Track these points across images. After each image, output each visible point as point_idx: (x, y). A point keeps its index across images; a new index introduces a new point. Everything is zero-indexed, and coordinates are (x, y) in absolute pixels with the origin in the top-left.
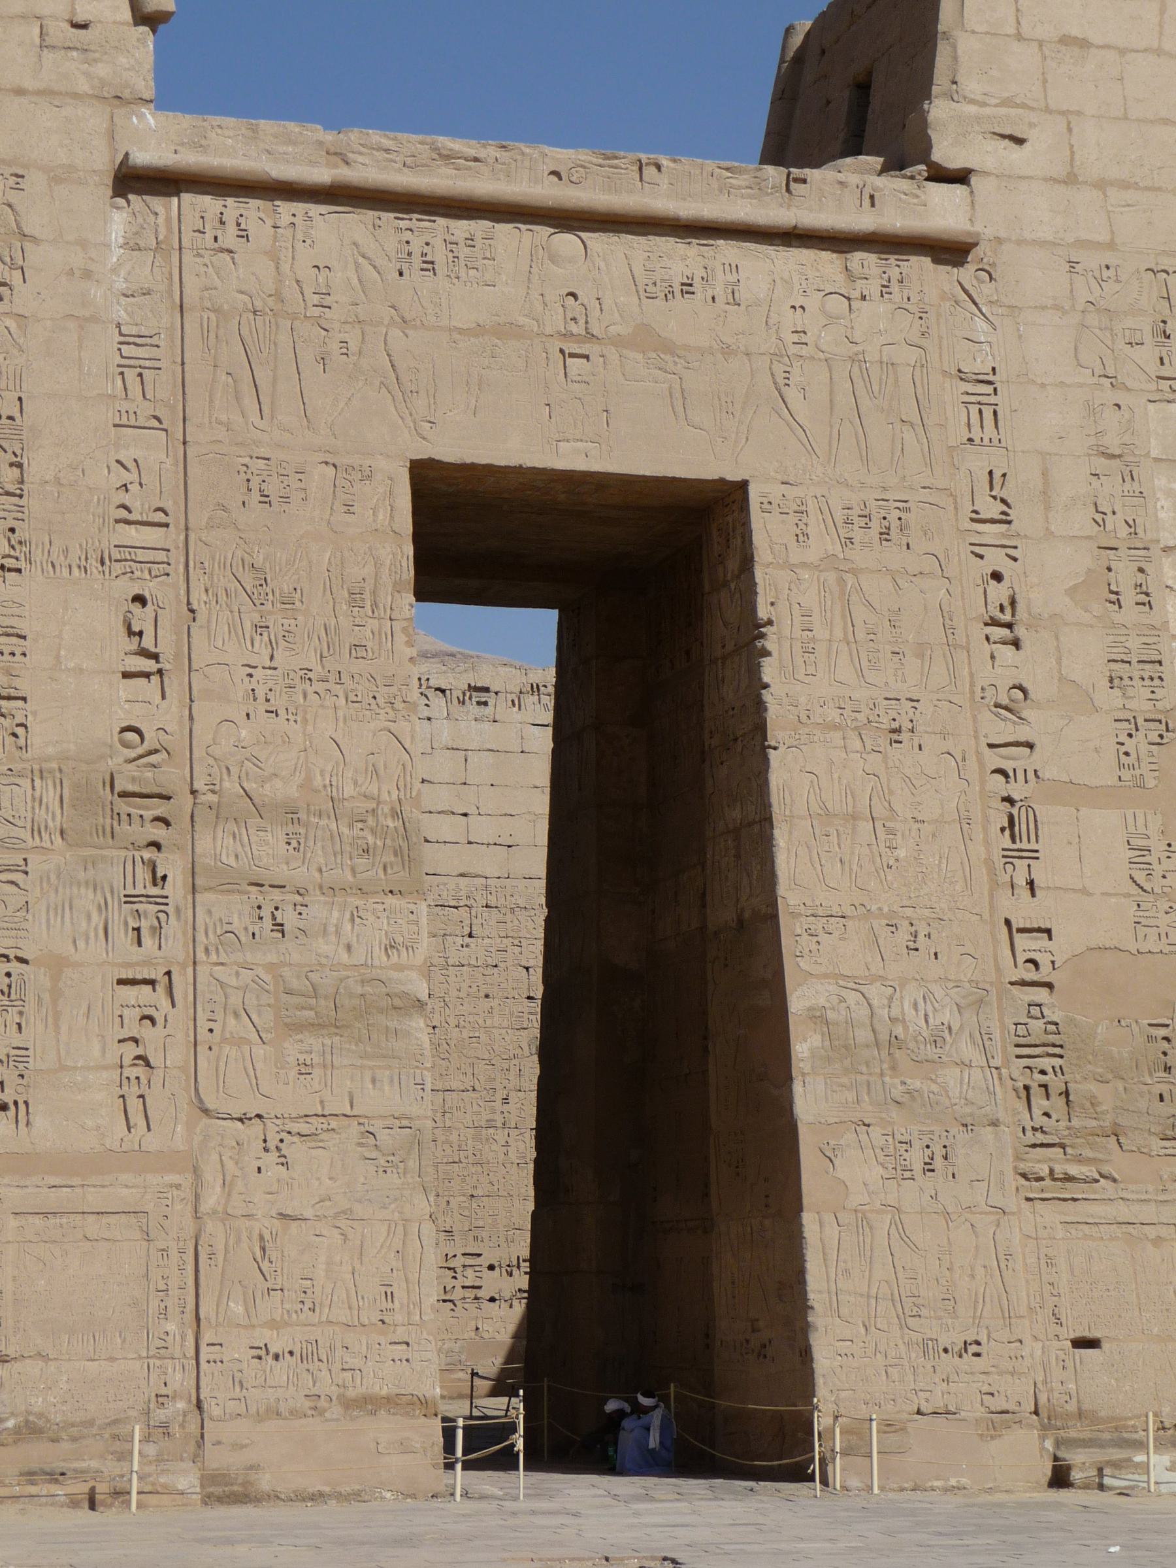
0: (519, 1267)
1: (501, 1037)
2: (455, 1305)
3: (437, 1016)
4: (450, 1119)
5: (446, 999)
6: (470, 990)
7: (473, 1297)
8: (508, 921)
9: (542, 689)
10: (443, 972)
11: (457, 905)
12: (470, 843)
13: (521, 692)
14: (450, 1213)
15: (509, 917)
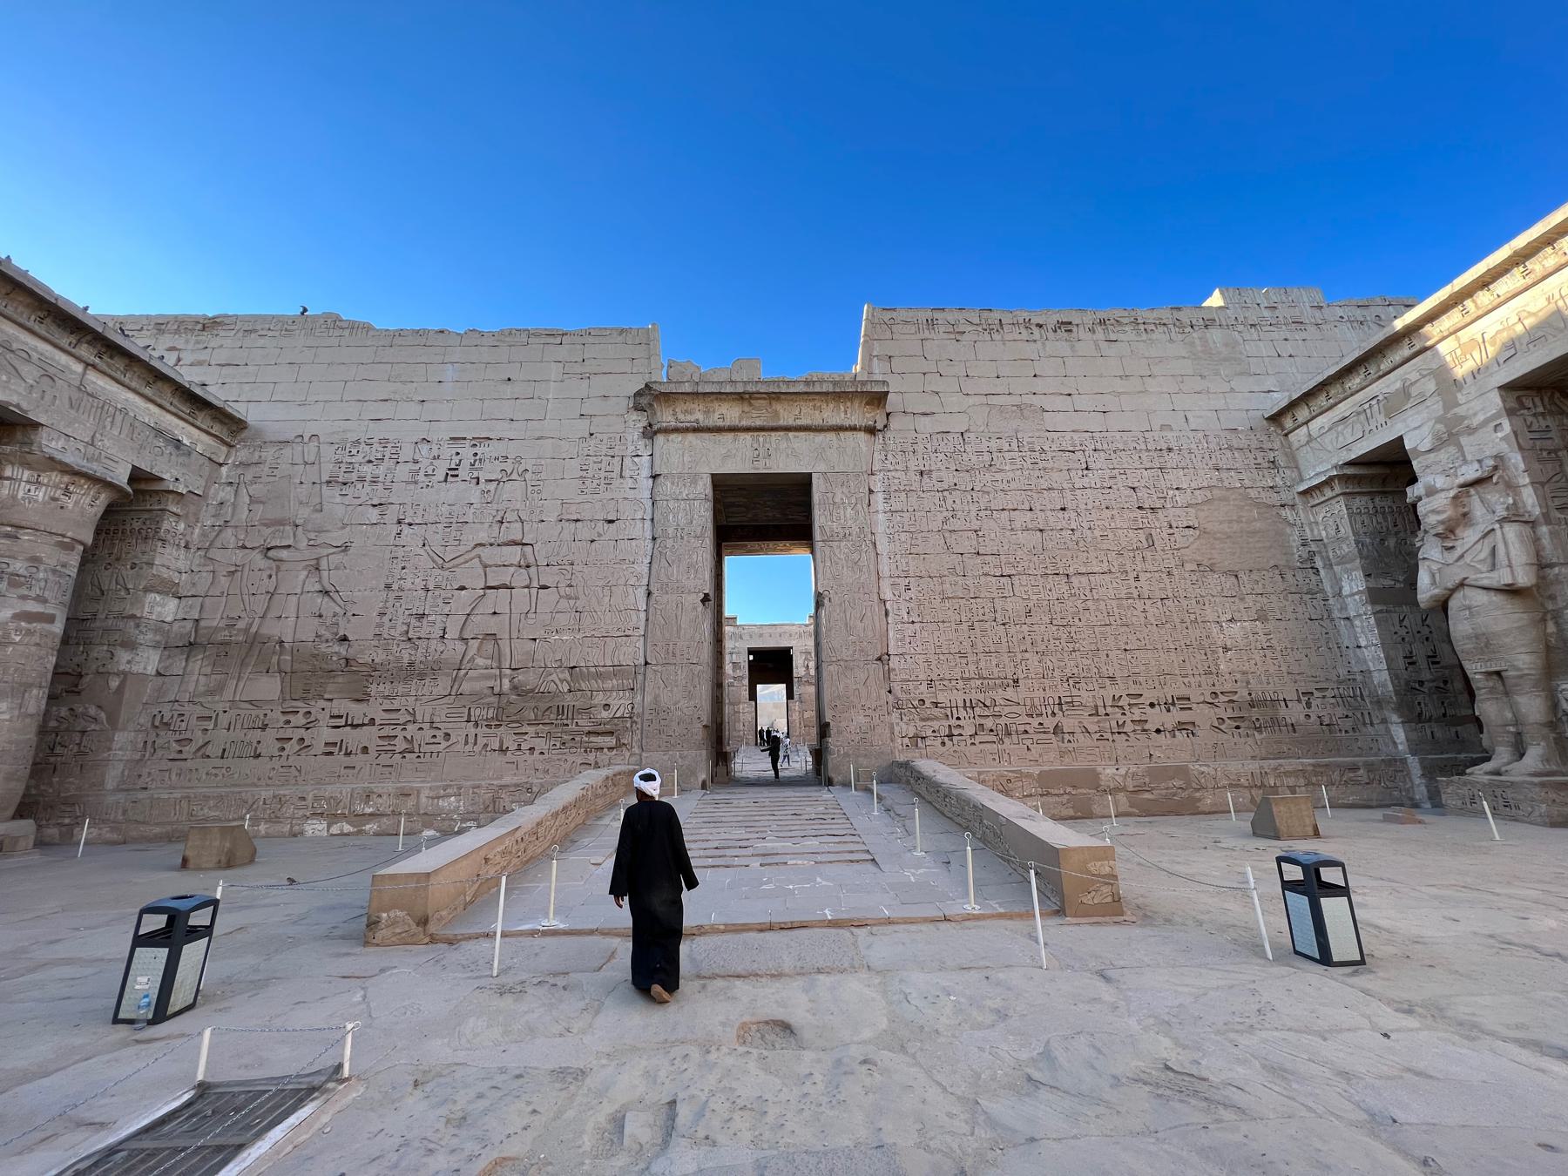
3: (1073, 522)
9: (1107, 322)
15: (1113, 456)
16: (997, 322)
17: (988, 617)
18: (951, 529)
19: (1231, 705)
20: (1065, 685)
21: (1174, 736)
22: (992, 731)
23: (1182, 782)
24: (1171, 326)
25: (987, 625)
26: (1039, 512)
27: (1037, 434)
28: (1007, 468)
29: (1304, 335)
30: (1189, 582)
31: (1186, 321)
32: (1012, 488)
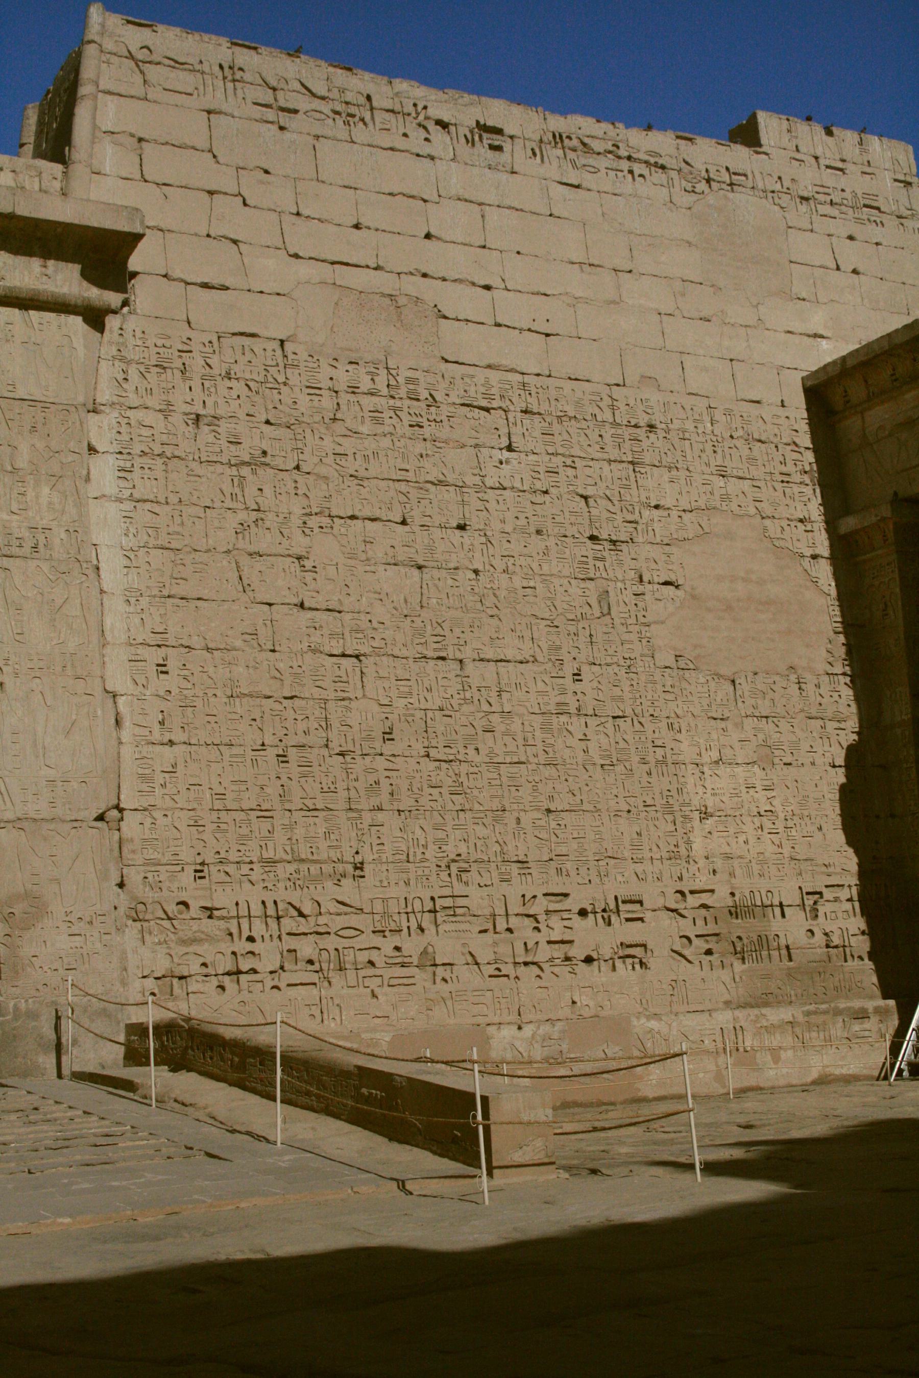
0: (618, 911)
1: (562, 589)
2: (542, 970)
3: (478, 555)
4: (509, 700)
5: (489, 533)
6: (518, 523)
7: (563, 956)
8: (556, 433)
9: (566, 141)
10: (479, 495)
11: (489, 406)
12: (498, 325)
13: (541, 141)
14: (522, 836)
15: (556, 427)
16: (362, 100)
17: (317, 738)
18: (252, 549)
19: (703, 912)
20: (444, 875)
21: (614, 968)
22: (311, 962)
23: (617, 1049)
24: (674, 174)
25: (313, 755)
26: (417, 529)
27: (425, 365)
28: (364, 429)
29: (876, 233)
30: (660, 688)
31: (699, 165)
32: (372, 473)
